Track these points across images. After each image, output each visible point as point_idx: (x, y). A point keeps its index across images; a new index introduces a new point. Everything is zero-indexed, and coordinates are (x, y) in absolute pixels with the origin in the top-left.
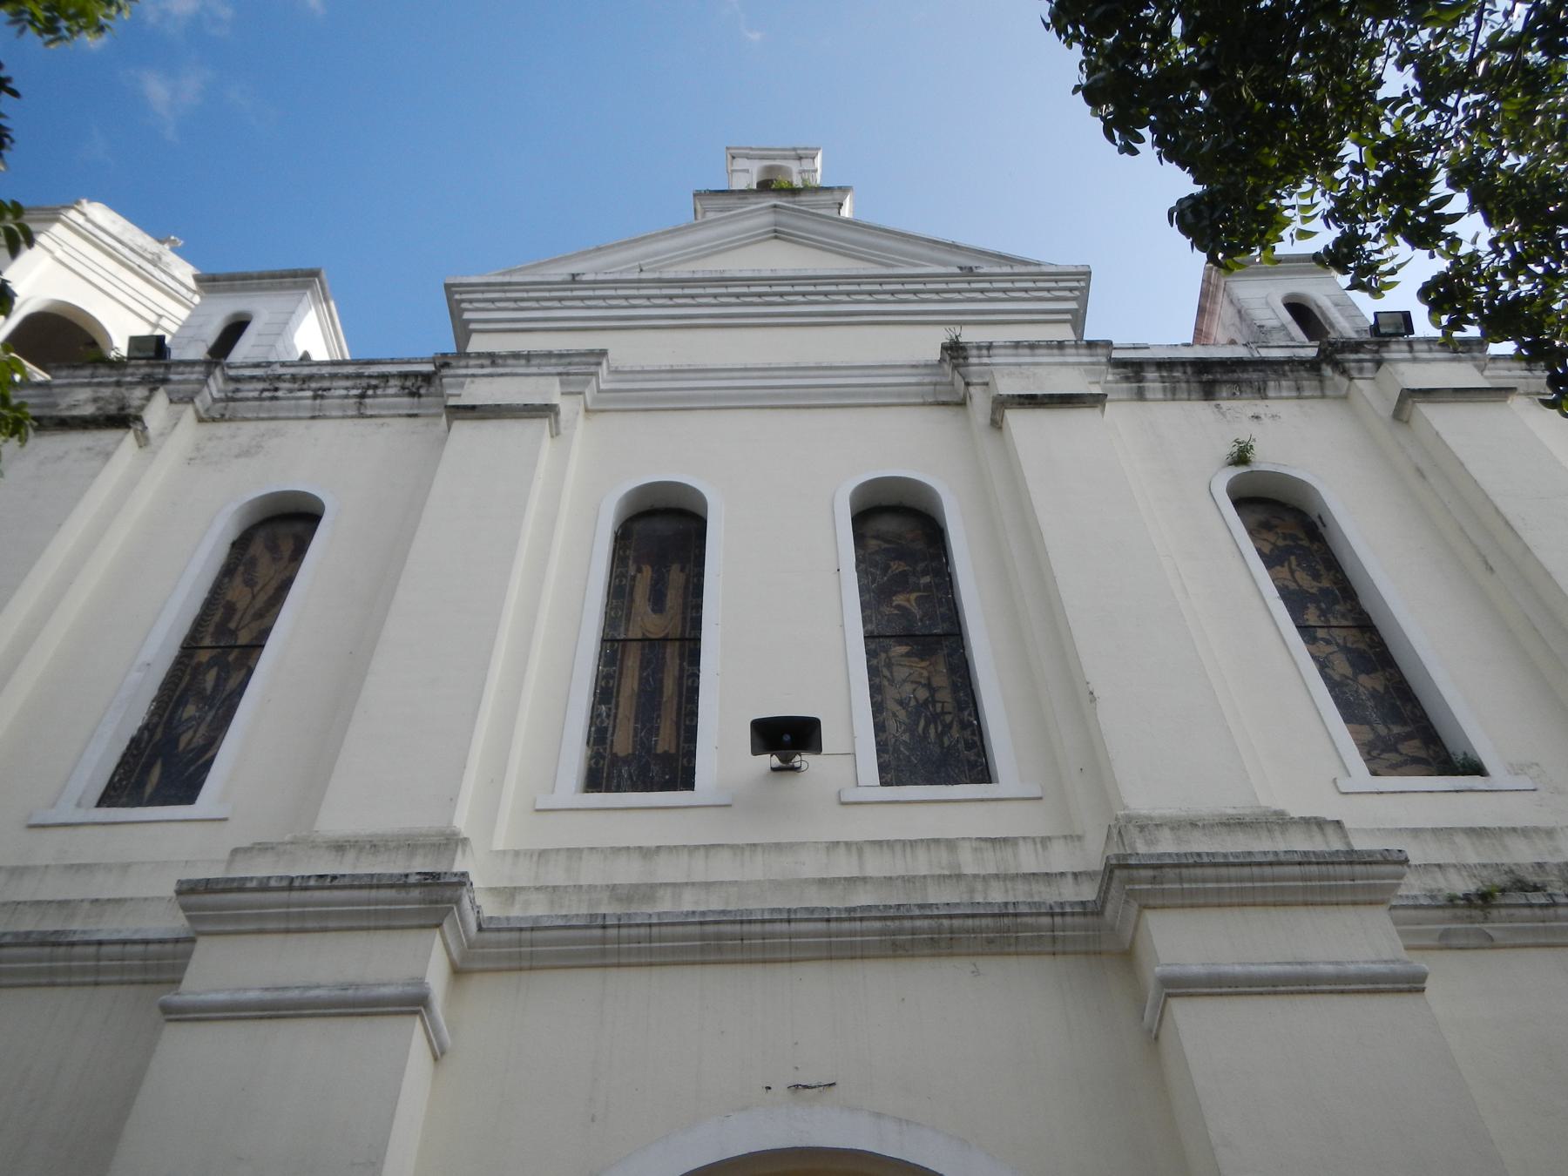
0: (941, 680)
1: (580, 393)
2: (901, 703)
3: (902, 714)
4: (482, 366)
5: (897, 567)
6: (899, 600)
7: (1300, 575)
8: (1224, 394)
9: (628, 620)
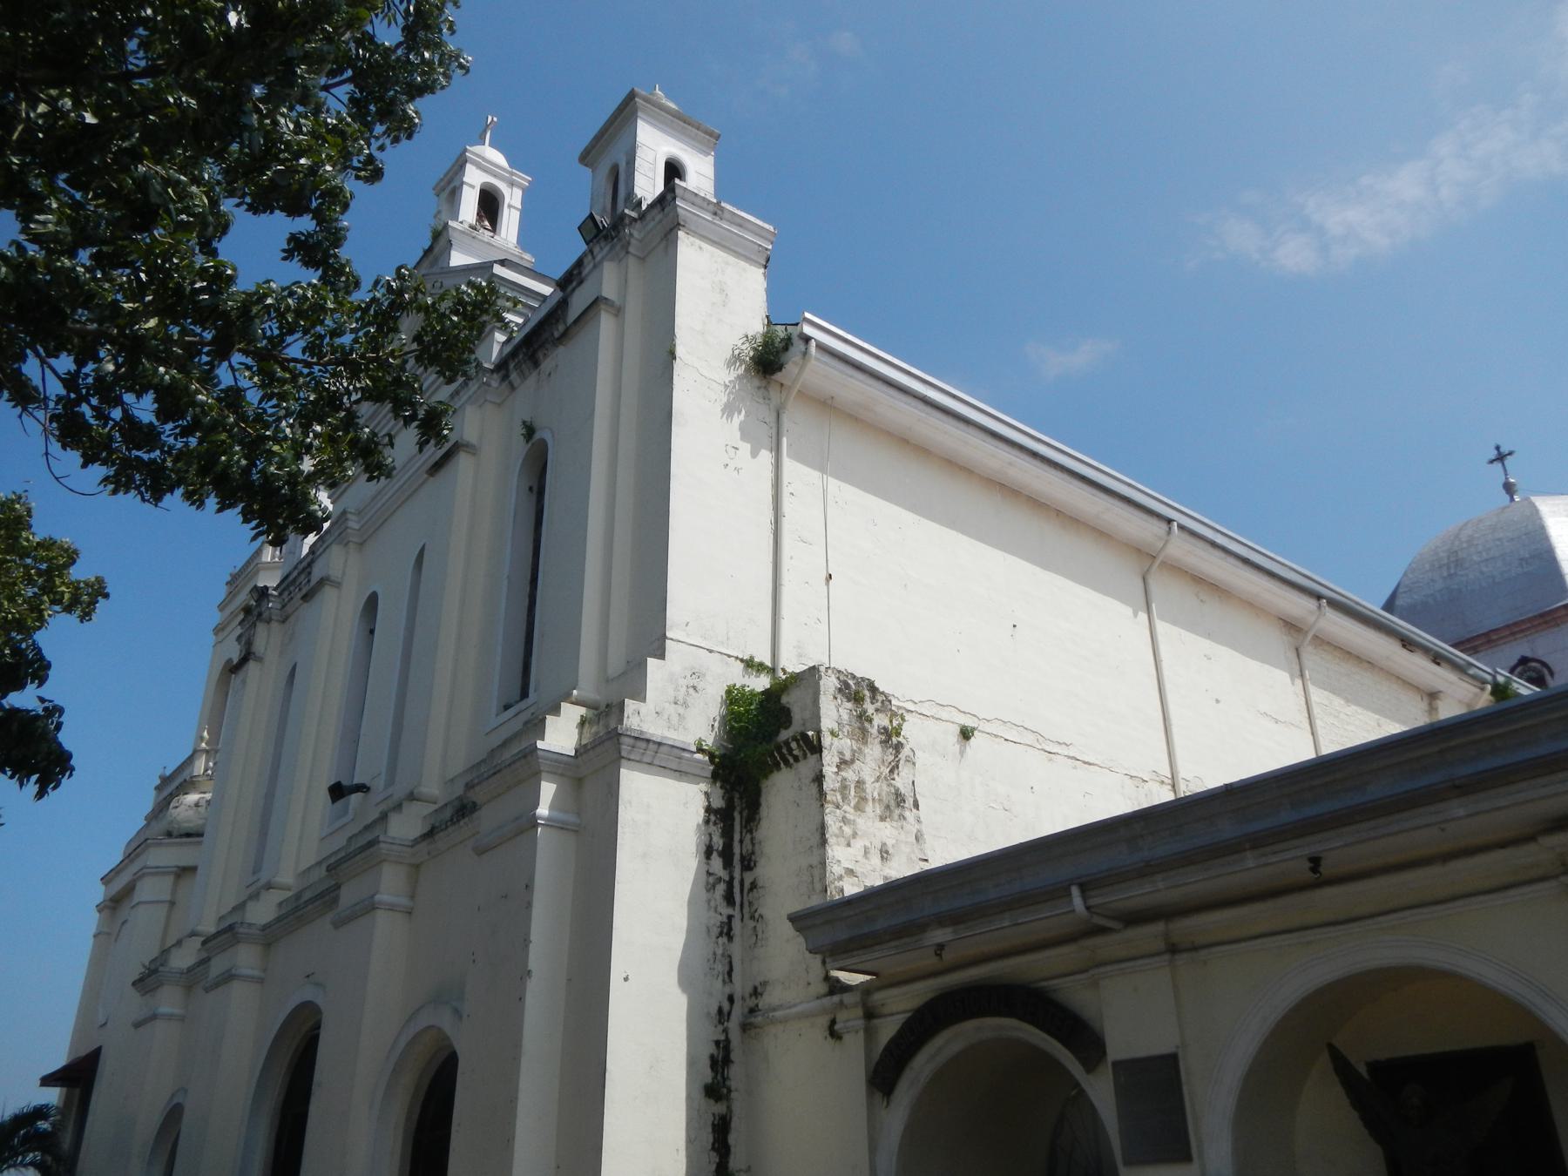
1: (349, 542)
4: (321, 546)
8: (541, 357)
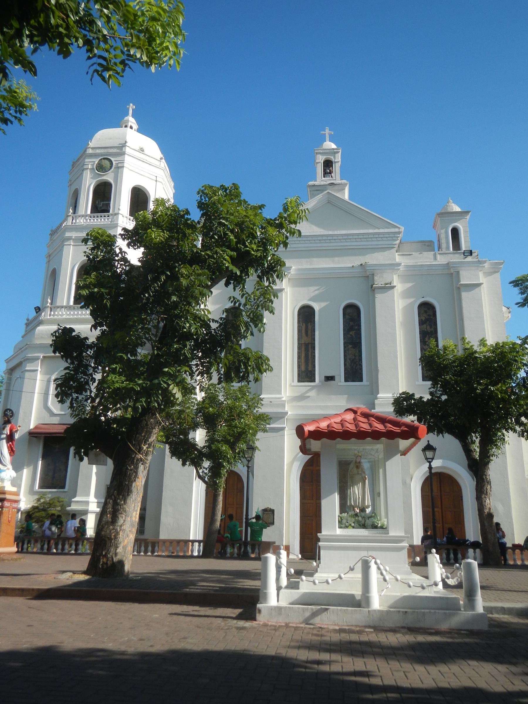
0: (357, 354)
2: (350, 359)
3: (349, 361)
5: (351, 323)
6: (351, 333)
7: (428, 327)
9: (302, 338)
